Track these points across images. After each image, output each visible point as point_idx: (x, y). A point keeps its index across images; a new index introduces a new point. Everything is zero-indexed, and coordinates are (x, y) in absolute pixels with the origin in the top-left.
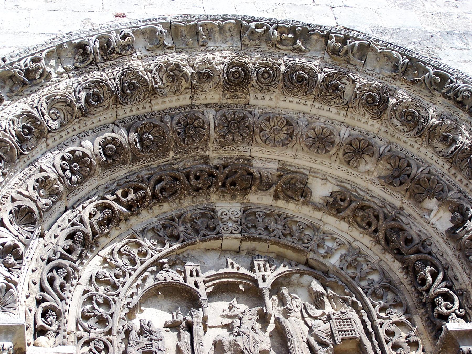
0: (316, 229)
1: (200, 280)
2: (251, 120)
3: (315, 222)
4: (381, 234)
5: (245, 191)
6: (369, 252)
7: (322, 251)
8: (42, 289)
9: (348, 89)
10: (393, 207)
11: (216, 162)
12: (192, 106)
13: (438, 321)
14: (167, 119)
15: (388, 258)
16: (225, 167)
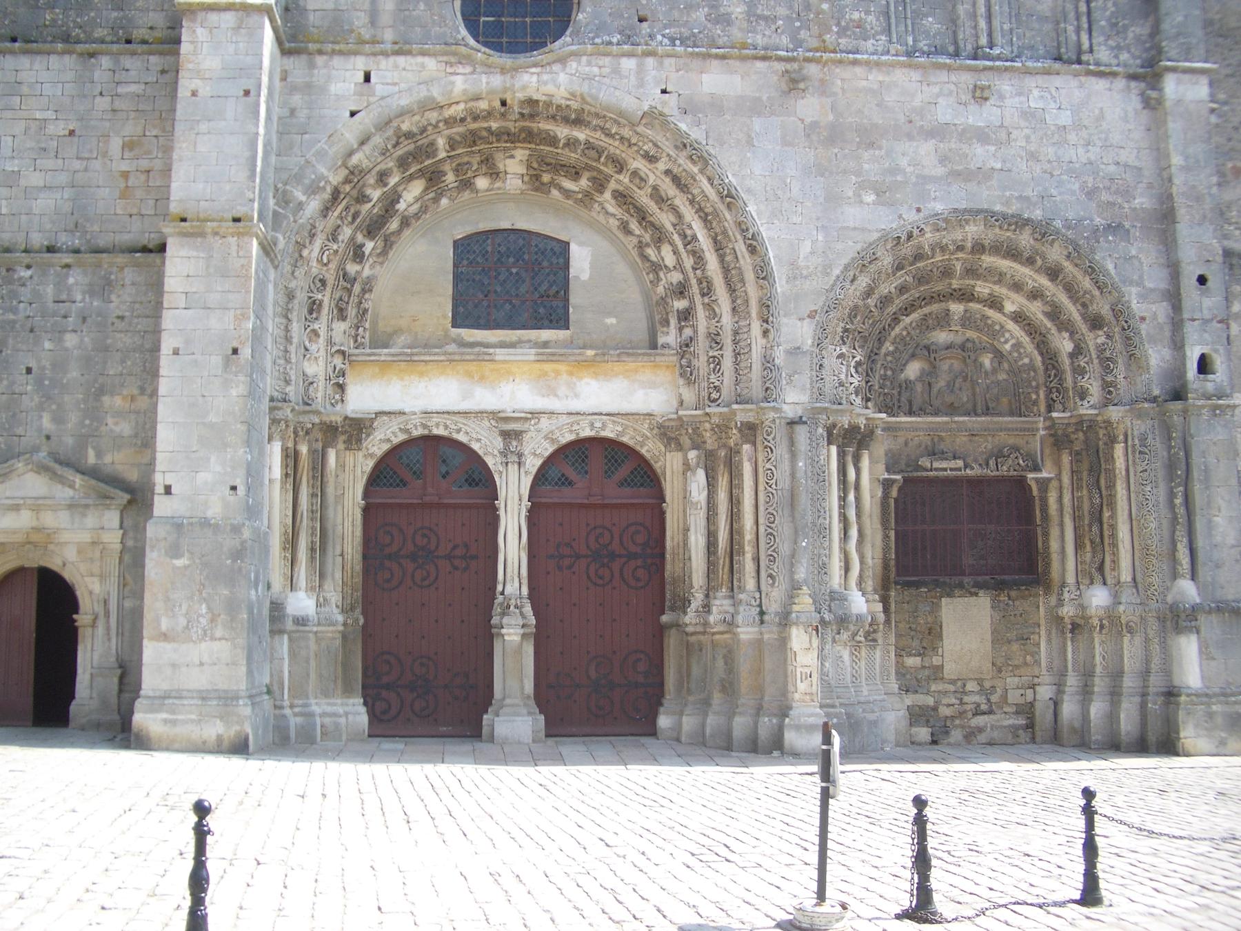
0: (1002, 327)
1: (937, 356)
2: (980, 271)
3: (1002, 321)
4: (1036, 341)
5: (970, 301)
6: (1027, 346)
7: (1002, 340)
8: (868, 375)
9: (1039, 262)
10: (1046, 328)
11: (954, 286)
12: (949, 260)
13: (1051, 402)
14: (935, 270)
15: (1036, 352)
16: (960, 290)
